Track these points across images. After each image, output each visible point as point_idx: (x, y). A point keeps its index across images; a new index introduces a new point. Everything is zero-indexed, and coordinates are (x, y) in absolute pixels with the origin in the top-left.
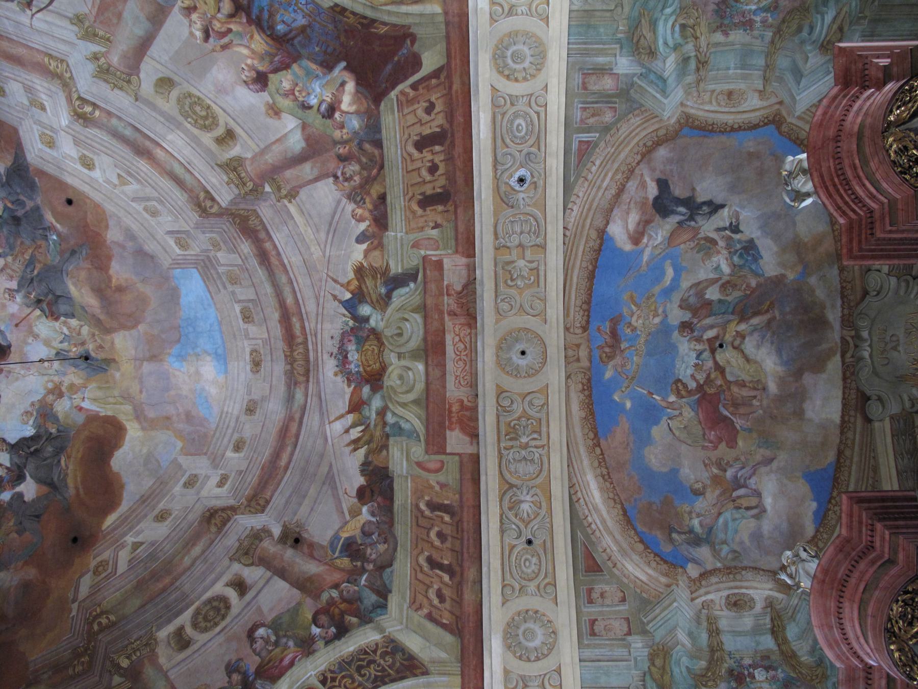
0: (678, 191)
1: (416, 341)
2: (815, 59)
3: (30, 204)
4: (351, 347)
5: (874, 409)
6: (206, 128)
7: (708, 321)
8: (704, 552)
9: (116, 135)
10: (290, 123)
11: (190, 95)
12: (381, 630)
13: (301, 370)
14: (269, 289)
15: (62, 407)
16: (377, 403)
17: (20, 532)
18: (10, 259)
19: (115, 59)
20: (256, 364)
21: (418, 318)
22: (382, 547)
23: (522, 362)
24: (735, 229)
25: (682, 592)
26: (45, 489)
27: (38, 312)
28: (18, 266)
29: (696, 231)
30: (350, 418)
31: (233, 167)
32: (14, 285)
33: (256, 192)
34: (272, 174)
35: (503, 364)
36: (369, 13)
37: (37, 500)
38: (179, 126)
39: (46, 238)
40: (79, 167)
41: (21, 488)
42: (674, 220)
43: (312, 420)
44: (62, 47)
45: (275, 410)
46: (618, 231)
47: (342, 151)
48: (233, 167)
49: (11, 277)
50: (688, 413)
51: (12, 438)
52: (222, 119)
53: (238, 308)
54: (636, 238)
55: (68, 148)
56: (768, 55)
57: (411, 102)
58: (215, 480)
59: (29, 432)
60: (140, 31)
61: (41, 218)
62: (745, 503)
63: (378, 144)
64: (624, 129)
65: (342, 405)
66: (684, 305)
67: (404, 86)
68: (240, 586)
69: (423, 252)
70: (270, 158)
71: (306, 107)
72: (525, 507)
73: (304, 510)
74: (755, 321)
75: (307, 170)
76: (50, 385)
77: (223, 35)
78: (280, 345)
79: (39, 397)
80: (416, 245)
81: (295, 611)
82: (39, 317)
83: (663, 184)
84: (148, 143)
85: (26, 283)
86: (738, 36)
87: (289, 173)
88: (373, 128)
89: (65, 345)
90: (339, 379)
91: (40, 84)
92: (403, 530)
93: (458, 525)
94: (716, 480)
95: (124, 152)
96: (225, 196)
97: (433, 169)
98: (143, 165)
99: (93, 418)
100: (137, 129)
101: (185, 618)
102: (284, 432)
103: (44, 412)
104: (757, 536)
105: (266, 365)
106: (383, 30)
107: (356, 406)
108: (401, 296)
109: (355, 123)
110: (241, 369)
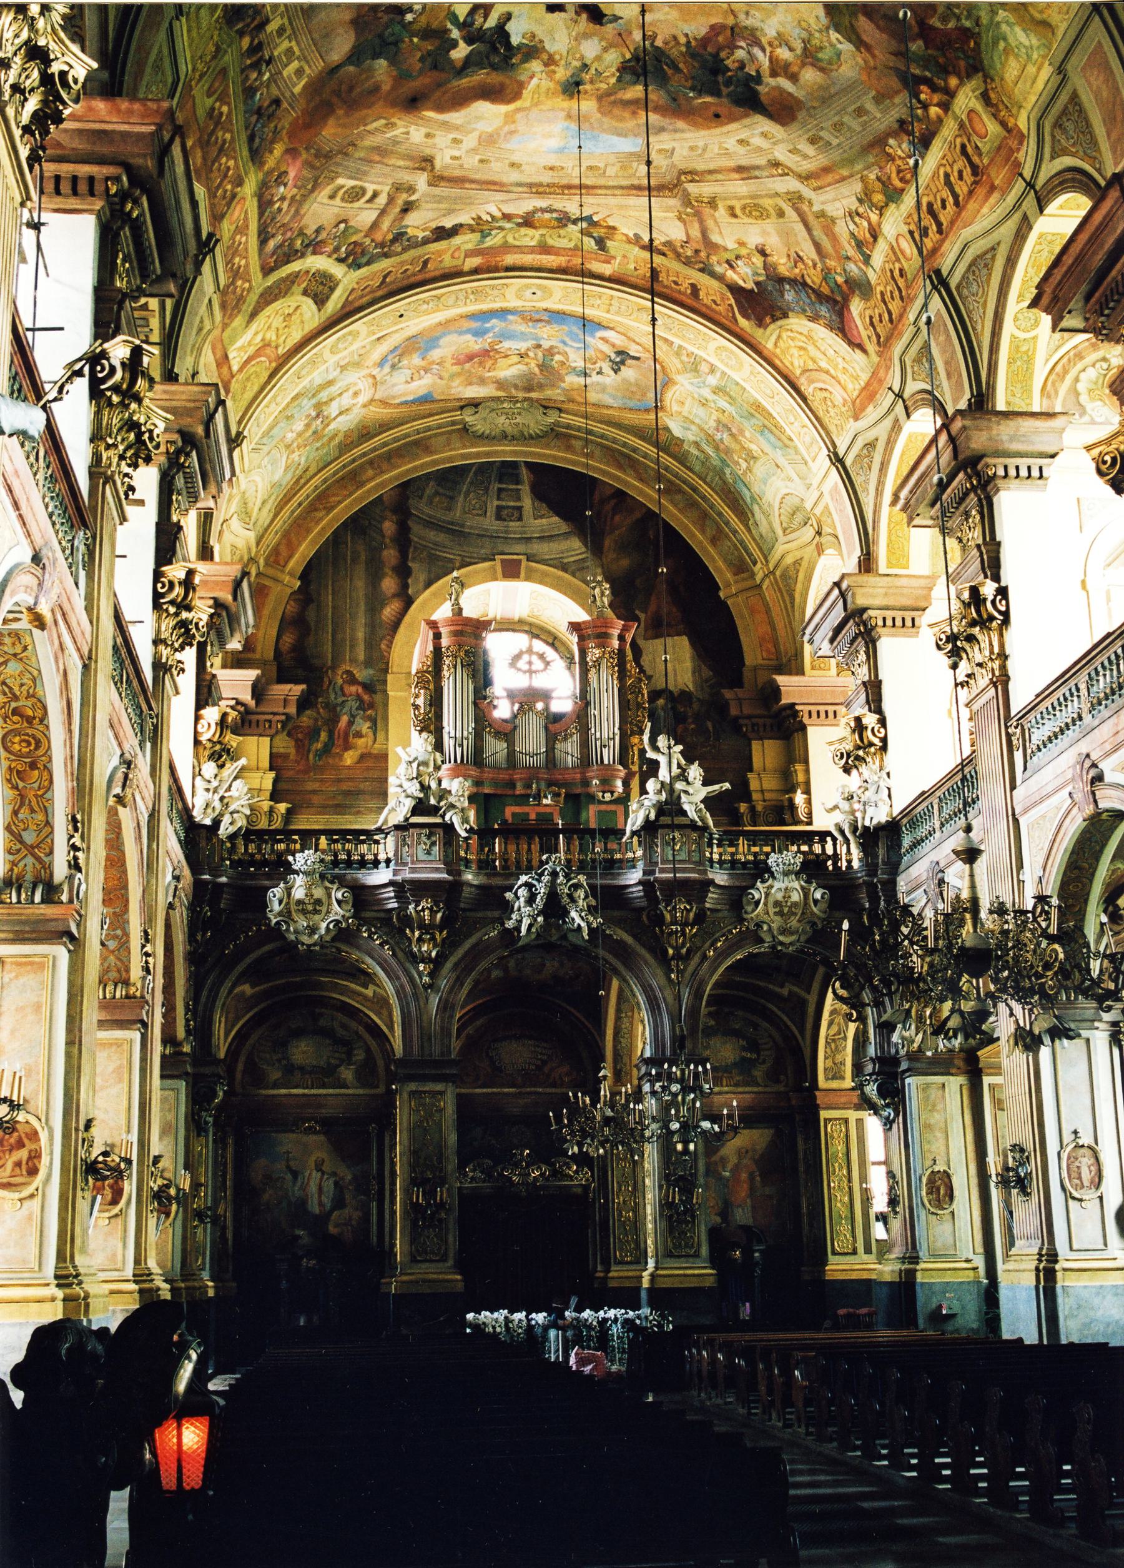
0: (629, 362)
1: (550, 242)
2: (692, 438)
3: (725, 91)
4: (555, 215)
5: (469, 411)
6: (744, 208)
7: (540, 354)
8: (387, 369)
9: (757, 168)
10: (731, 245)
11: (768, 216)
12: (346, 274)
13: (541, 189)
14: (611, 183)
15: (536, 66)
16: (508, 225)
17: (422, 59)
18: (683, 49)
19: (805, 207)
20: (551, 169)
21: (571, 245)
22: (399, 249)
23: (528, 293)
24: (600, 373)
25: (366, 372)
26: (459, 65)
27: (628, 56)
28: (674, 53)
29: (603, 360)
30: (498, 214)
31: (712, 203)
32: (659, 43)
33: (687, 201)
34: (698, 214)
35: (527, 286)
36: (779, 323)
37: (451, 62)
38: (752, 197)
39: (692, 89)
40: (742, 136)
41: (462, 44)
42: (613, 356)
43: (499, 196)
44: (822, 198)
45: (514, 176)
46: (609, 334)
47: (703, 254)
48: (712, 203)
49: (666, 43)
50: (477, 347)
51: (510, 27)
52: (746, 220)
53: (602, 165)
54: (602, 339)
55: (757, 141)
56: (699, 426)
57: (722, 299)
58: (457, 153)
59: (515, 40)
60: (815, 233)
61: (712, 94)
62: (416, 377)
63: (702, 270)
64: (676, 361)
65: (508, 209)
66: (552, 347)
67: (733, 302)
68: (375, 195)
69: (618, 259)
70: (710, 223)
71: (738, 257)
72: (425, 306)
73: (430, 206)
74: (537, 370)
75: (695, 232)
76: (557, 57)
77: (796, 263)
78: (564, 182)
79: (547, 47)
80: (624, 256)
81: (357, 231)
82: (623, 56)
83: (638, 359)
84: (745, 175)
85: (659, 55)
86: (713, 424)
87: (696, 225)
88: (713, 274)
89: (593, 71)
90: (531, 208)
91: (806, 166)
92: (413, 253)
93: (414, 275)
94: (433, 363)
95: (744, 162)
96: (692, 188)
97: (676, 283)
98: (732, 164)
99: (521, 86)
100: (756, 178)
101: (352, 183)
102: (495, 183)
103: (532, 51)
104: (394, 385)
105: (551, 173)
106: (768, 320)
107: (507, 217)
108: (590, 244)
109: (719, 269)
110: (552, 161)
